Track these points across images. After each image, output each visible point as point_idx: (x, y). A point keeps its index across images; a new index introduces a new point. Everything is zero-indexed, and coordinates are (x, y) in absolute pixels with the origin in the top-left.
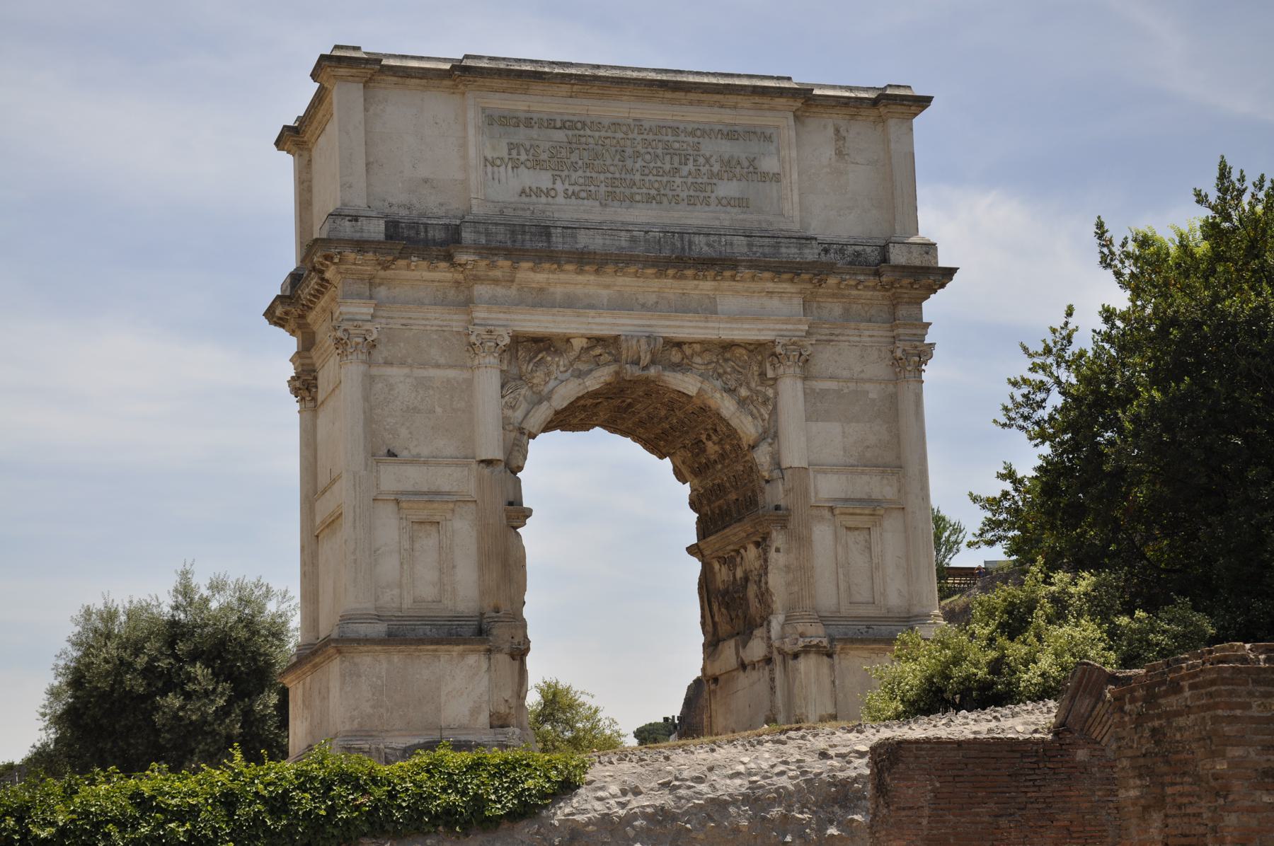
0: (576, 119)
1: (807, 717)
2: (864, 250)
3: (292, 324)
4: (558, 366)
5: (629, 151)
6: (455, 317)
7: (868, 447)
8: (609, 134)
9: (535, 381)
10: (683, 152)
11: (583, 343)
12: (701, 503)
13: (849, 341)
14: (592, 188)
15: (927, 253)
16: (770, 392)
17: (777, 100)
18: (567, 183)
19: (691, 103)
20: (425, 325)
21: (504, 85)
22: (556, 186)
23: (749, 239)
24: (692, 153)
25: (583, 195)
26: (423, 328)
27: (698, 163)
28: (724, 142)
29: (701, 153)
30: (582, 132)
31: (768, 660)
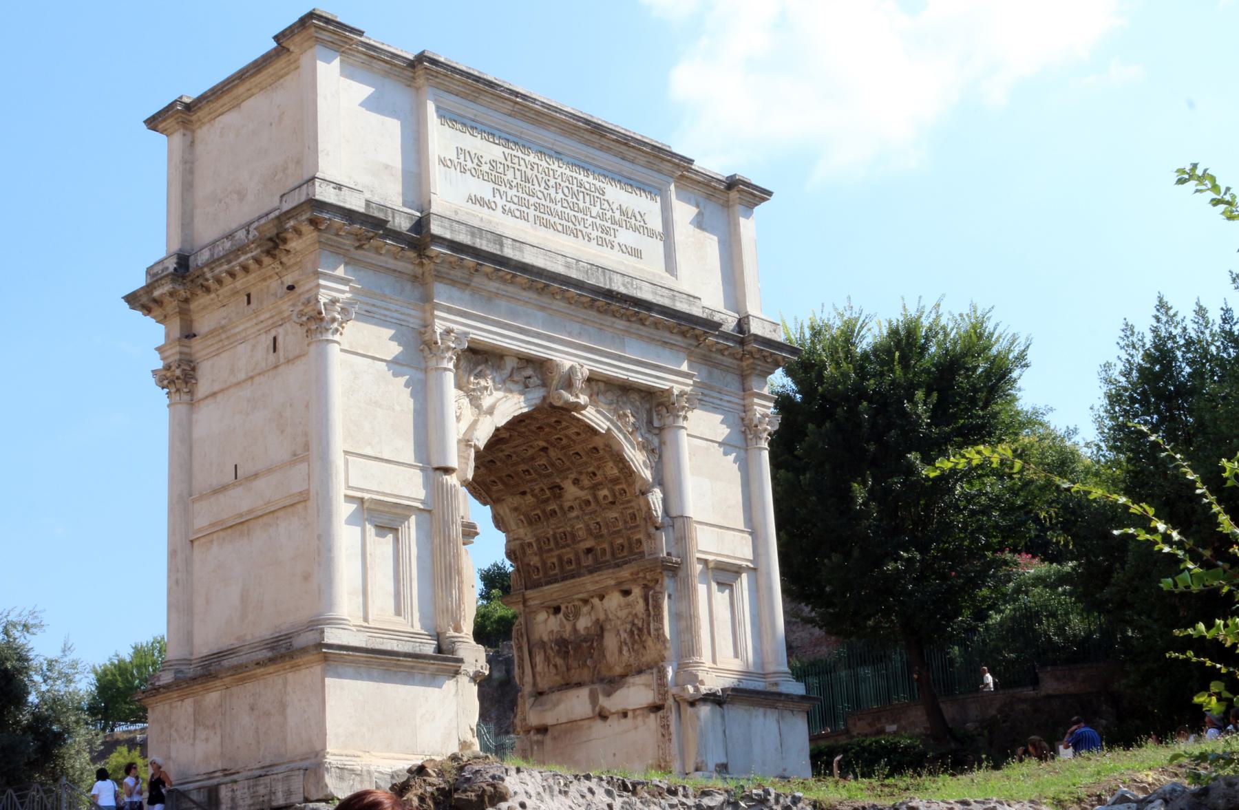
1: (707, 765)
2: (727, 319)
3: (172, 305)
5: (552, 183)
6: (413, 312)
12: (524, 553)
13: (713, 403)
14: (524, 209)
15: (775, 331)
18: (504, 197)
19: (601, 148)
20: (386, 316)
21: (460, 88)
23: (653, 287)
25: (518, 214)
26: (383, 318)
29: (606, 197)
31: (656, 708)
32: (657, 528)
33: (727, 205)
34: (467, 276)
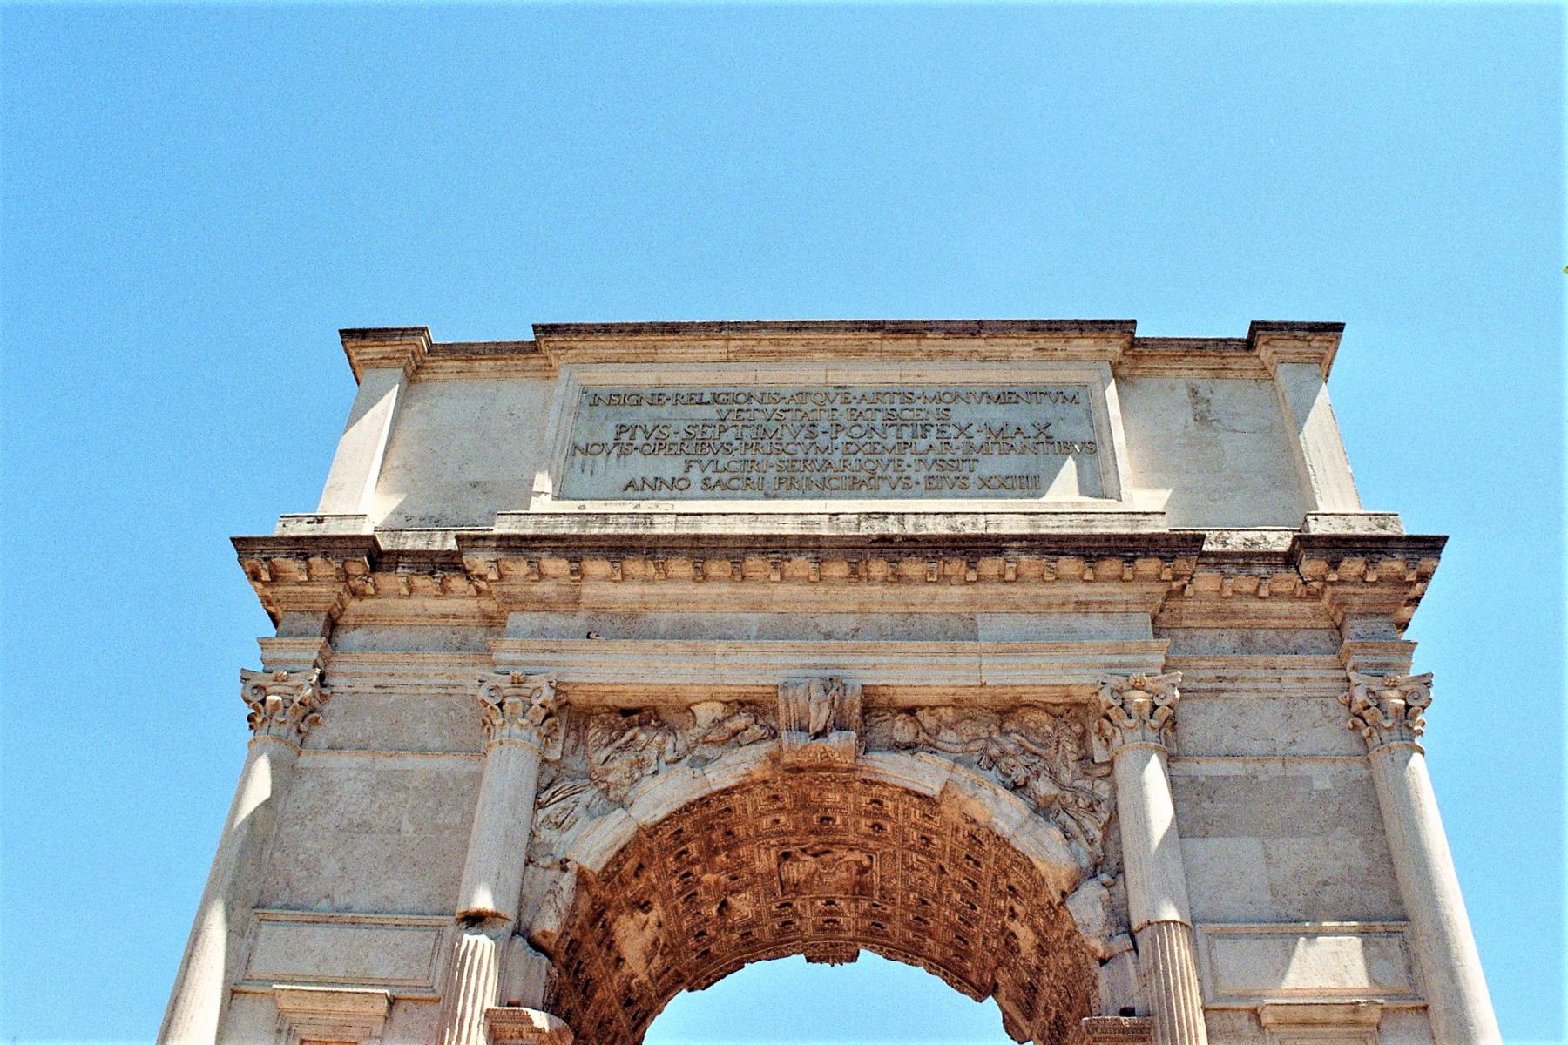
0: (739, 390)
2: (1264, 538)
4: (661, 753)
5: (824, 424)
7: (1326, 883)
8: (792, 405)
9: (610, 779)
10: (919, 423)
11: (718, 710)
16: (1103, 789)
17: (1076, 342)
19: (930, 356)
21: (619, 351)
22: (688, 475)
24: (934, 422)
26: (413, 691)
27: (946, 435)
28: (992, 406)
29: (951, 421)
30: (745, 407)
32: (1103, 962)
33: (1266, 375)
34: (568, 589)
